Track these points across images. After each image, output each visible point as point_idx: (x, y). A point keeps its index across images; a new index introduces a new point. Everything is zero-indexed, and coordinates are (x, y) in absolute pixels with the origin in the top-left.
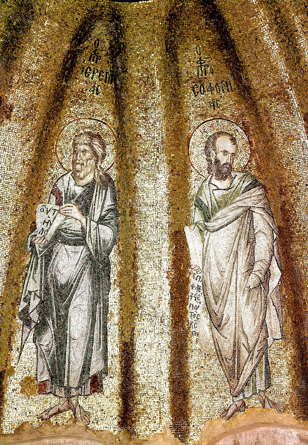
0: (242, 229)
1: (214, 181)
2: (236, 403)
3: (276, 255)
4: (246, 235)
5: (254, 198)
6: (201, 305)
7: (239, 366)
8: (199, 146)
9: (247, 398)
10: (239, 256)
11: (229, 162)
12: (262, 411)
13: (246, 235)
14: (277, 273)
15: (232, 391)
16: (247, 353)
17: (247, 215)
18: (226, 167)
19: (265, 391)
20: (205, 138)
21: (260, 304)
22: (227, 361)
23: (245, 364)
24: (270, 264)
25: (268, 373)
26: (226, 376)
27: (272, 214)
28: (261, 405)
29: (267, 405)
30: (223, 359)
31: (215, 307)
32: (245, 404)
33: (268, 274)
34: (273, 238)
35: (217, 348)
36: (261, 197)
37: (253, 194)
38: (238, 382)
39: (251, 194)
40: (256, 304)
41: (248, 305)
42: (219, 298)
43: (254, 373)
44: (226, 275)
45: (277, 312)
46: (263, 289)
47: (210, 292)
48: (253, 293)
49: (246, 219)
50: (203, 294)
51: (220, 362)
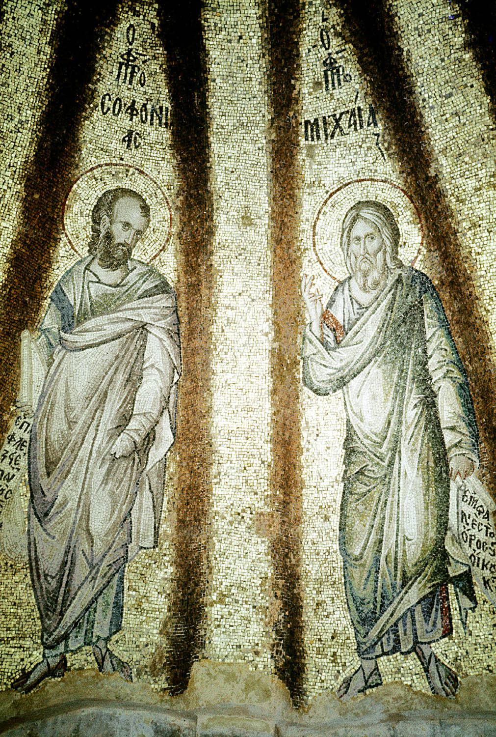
0: (123, 357)
1: (96, 267)
2: (50, 660)
3: (171, 409)
4: (129, 367)
5: (155, 310)
6: (18, 475)
7: (67, 592)
8: (85, 201)
9: (72, 651)
10: (107, 400)
11: (129, 242)
12: (97, 675)
13: (129, 367)
14: (166, 439)
15: (45, 637)
16: (87, 568)
17: (138, 336)
18: (122, 250)
19: (107, 640)
20: (98, 191)
21: (127, 485)
22: (46, 579)
23: (79, 588)
24: (158, 422)
25: (119, 607)
26: (39, 609)
27: (180, 342)
28: (96, 666)
29: (107, 665)
30: (39, 576)
31: (44, 482)
32: (66, 662)
33: (150, 437)
34: (173, 381)
35: (33, 554)
36: (167, 312)
37: (154, 305)
38: (61, 619)
39: (152, 303)
40: (120, 485)
41: (106, 484)
42: (56, 466)
43: (94, 605)
44: (77, 428)
45: (154, 502)
46: (137, 460)
47: (41, 452)
48: (119, 465)
49: (135, 341)
50: (27, 454)
51: (33, 580)
